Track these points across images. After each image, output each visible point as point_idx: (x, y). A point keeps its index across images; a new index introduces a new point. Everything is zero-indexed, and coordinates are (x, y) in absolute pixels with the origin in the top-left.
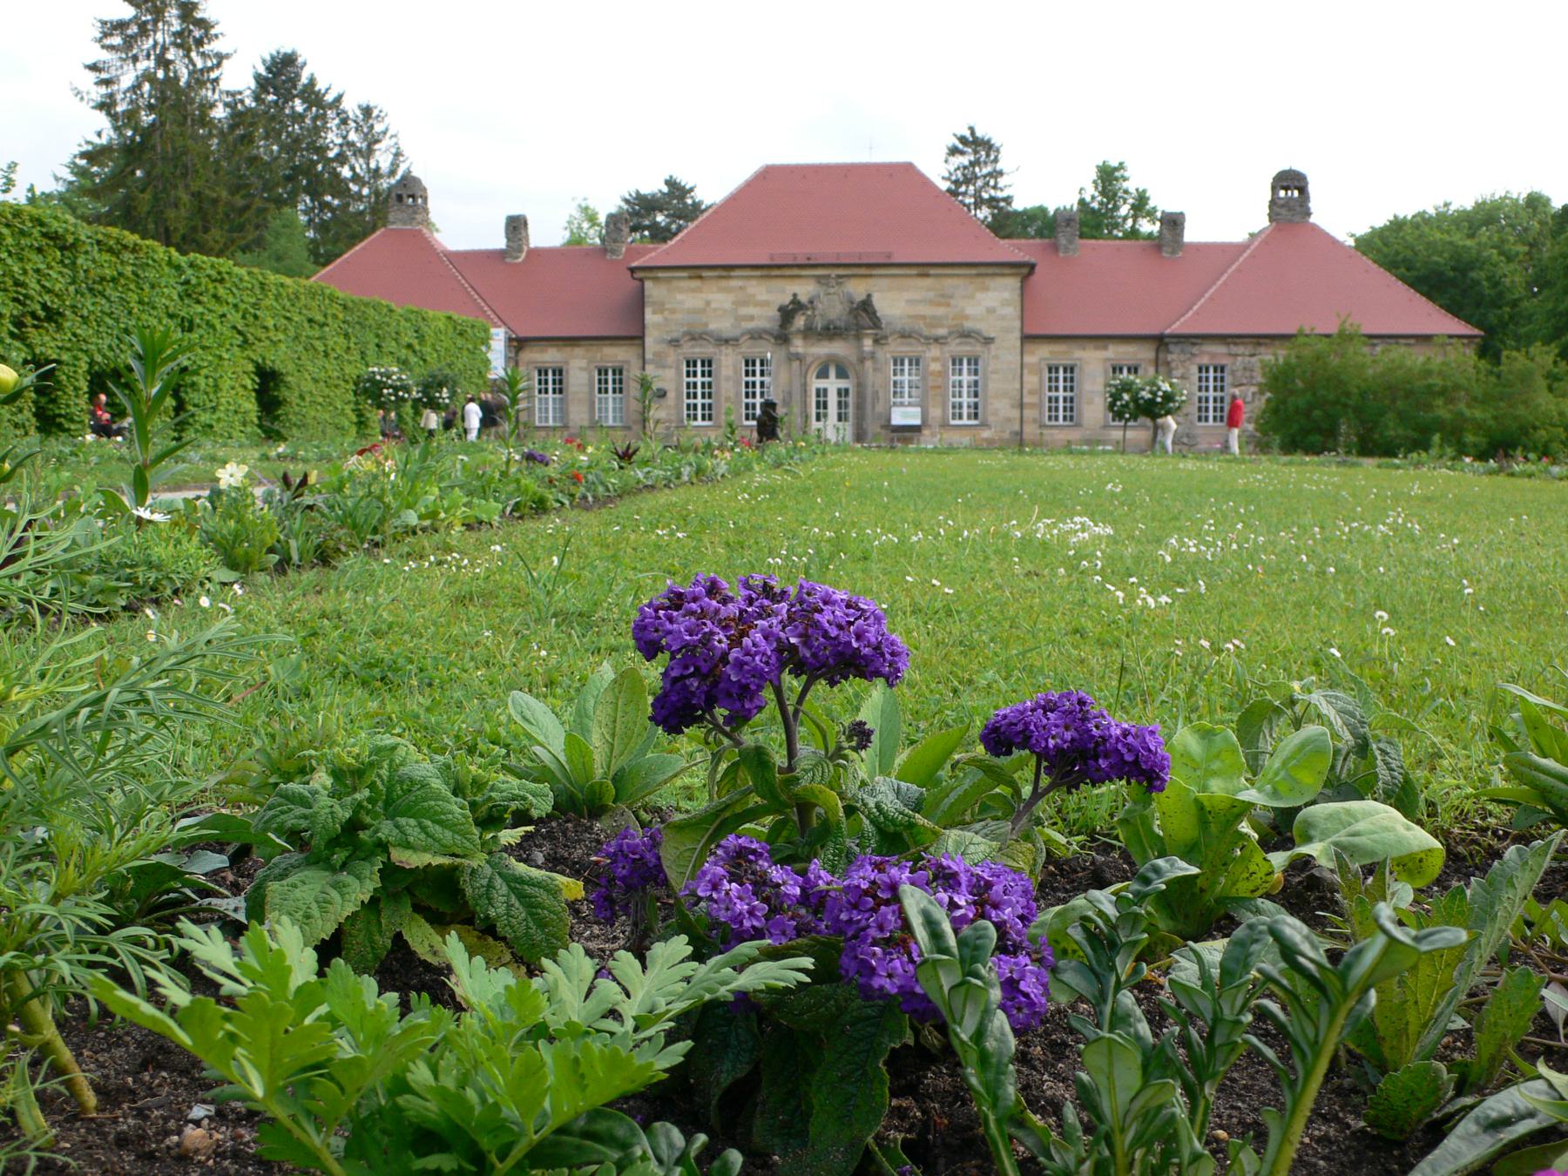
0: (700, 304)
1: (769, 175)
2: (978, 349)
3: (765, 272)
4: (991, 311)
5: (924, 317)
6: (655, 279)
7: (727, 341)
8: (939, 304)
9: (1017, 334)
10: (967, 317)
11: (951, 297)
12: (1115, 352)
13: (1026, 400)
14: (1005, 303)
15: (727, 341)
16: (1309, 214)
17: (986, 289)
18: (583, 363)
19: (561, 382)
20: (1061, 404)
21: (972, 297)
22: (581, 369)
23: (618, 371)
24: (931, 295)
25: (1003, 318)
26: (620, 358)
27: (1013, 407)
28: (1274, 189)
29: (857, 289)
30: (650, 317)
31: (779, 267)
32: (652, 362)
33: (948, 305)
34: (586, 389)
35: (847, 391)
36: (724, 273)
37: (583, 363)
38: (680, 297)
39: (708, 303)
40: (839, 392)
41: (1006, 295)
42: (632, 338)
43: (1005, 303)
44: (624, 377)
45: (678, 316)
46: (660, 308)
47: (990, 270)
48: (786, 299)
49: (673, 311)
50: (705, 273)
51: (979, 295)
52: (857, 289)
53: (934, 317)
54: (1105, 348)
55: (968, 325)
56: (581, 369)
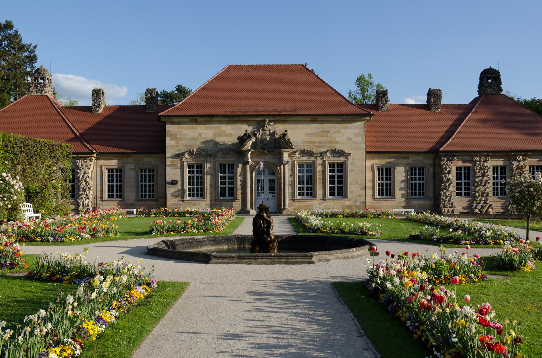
0: (196, 136)
1: (231, 70)
2: (342, 159)
3: (230, 119)
4: (350, 139)
5: (314, 142)
6: (172, 123)
7: (210, 155)
8: (323, 136)
9: (363, 152)
10: (337, 143)
11: (329, 132)
12: (412, 159)
13: (367, 185)
14: (356, 135)
15: (210, 155)
16: (501, 90)
17: (347, 128)
18: (133, 166)
19: (120, 176)
20: (385, 187)
21: (339, 132)
22: (131, 169)
23: (152, 171)
24: (318, 131)
25: (356, 142)
26: (152, 164)
27: (361, 189)
28: (481, 78)
29: (279, 129)
30: (169, 142)
31: (238, 116)
32: (170, 165)
33: (327, 136)
34: (134, 180)
35: (274, 180)
36: (209, 120)
37: (133, 166)
38: (185, 131)
39: (200, 135)
40: (270, 180)
41: (357, 131)
42: (160, 153)
43: (356, 135)
44: (155, 173)
45: (184, 142)
46: (174, 137)
47: (349, 118)
48: (242, 133)
49: (181, 139)
50: (199, 119)
51: (343, 131)
52: (279, 129)
53: (320, 143)
54: (408, 158)
55: (338, 147)
56: (131, 169)
